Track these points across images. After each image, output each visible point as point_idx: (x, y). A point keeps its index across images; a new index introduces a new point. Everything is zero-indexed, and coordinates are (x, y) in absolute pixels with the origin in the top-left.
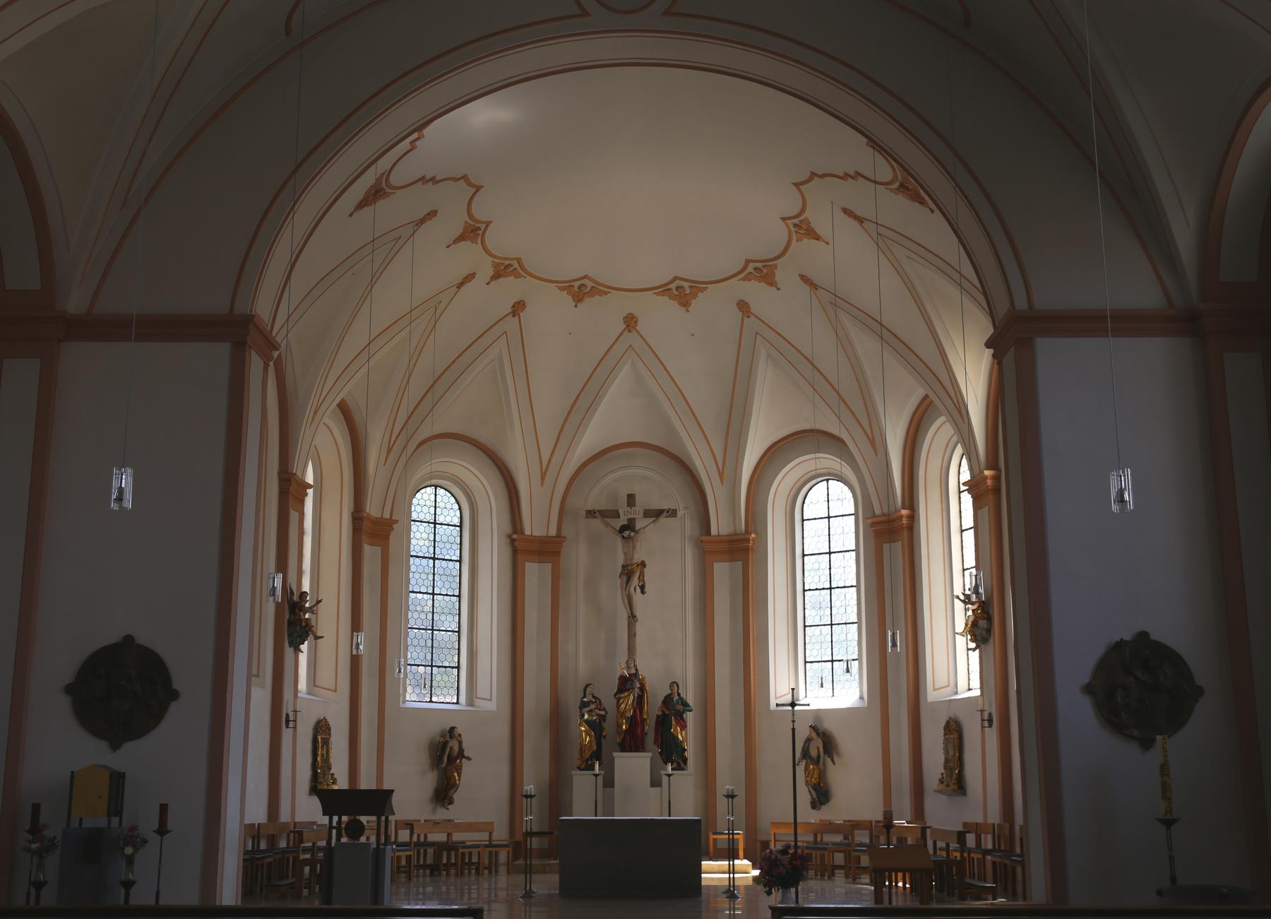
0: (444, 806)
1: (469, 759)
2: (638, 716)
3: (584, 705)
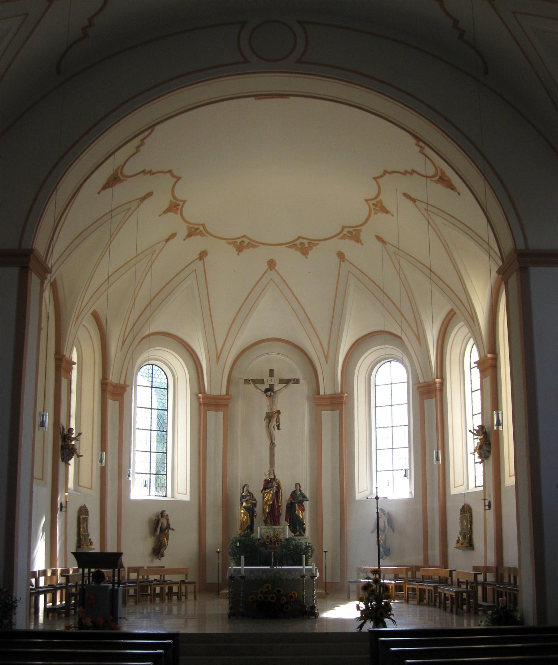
0: (158, 558)
1: (173, 530)
3: (242, 497)
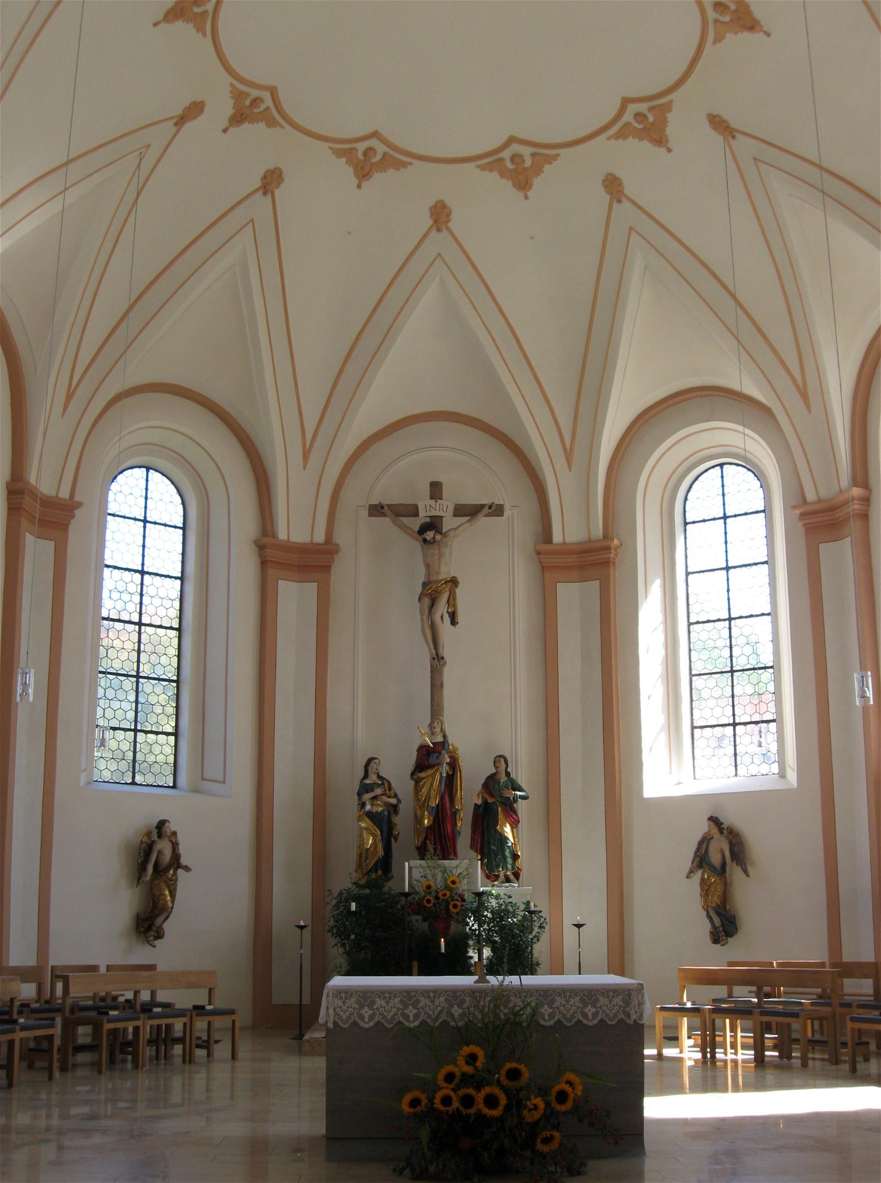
0: (148, 942)
1: (187, 869)
2: (448, 806)
3: (364, 789)
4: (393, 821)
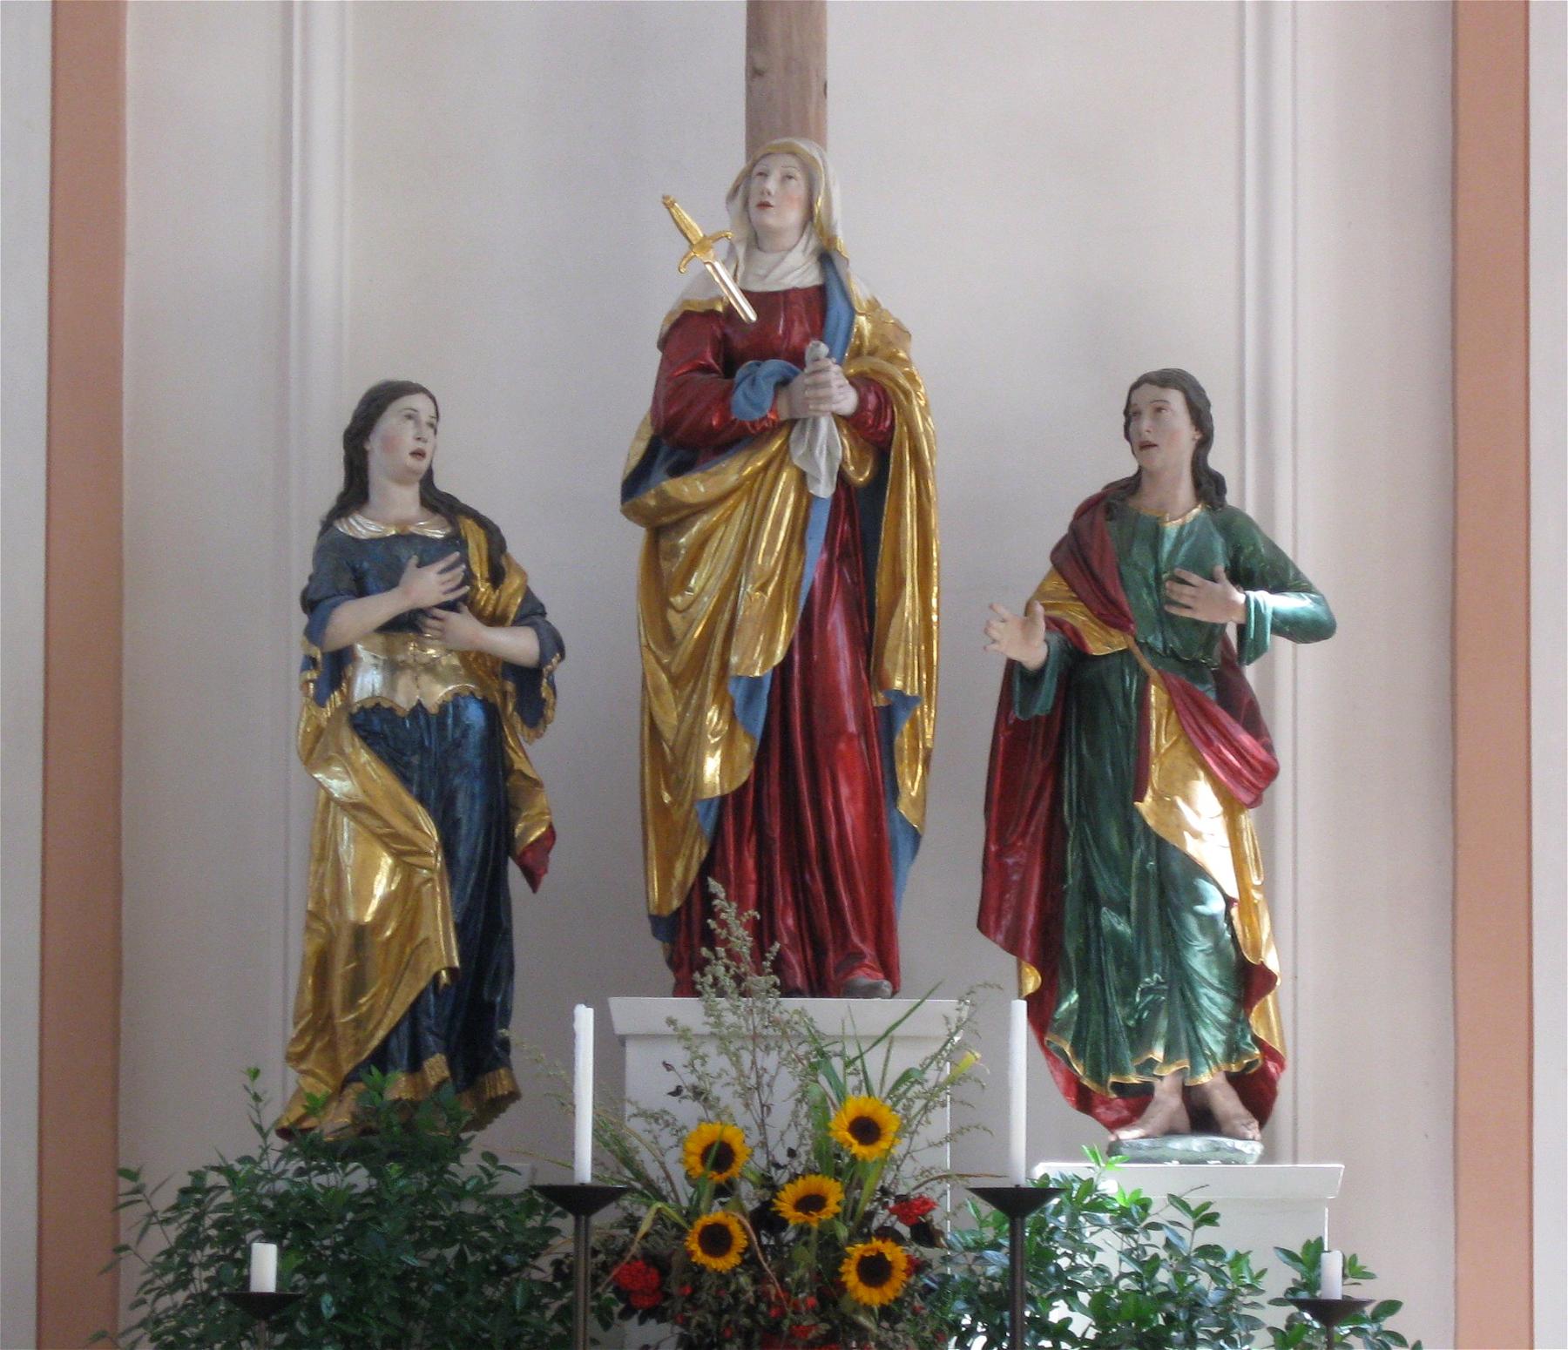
2: (844, 668)
4: (519, 764)
